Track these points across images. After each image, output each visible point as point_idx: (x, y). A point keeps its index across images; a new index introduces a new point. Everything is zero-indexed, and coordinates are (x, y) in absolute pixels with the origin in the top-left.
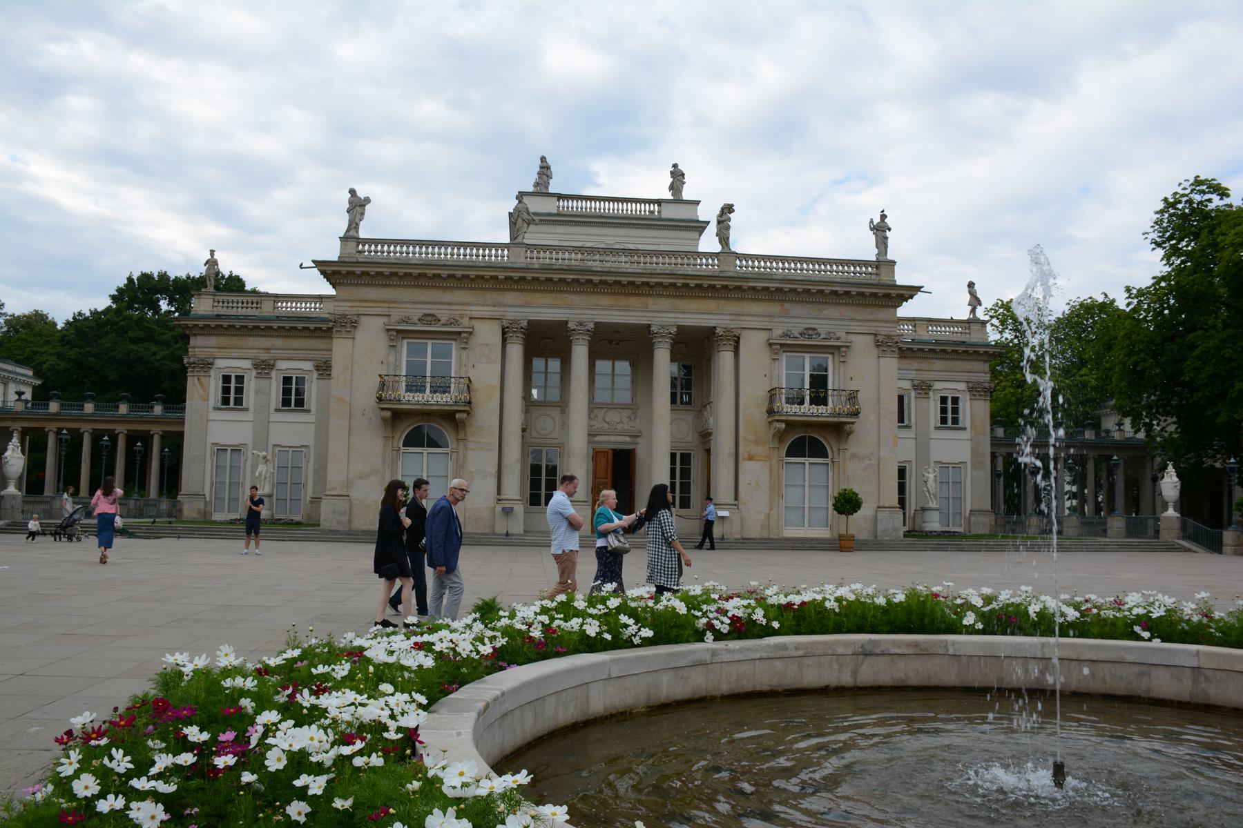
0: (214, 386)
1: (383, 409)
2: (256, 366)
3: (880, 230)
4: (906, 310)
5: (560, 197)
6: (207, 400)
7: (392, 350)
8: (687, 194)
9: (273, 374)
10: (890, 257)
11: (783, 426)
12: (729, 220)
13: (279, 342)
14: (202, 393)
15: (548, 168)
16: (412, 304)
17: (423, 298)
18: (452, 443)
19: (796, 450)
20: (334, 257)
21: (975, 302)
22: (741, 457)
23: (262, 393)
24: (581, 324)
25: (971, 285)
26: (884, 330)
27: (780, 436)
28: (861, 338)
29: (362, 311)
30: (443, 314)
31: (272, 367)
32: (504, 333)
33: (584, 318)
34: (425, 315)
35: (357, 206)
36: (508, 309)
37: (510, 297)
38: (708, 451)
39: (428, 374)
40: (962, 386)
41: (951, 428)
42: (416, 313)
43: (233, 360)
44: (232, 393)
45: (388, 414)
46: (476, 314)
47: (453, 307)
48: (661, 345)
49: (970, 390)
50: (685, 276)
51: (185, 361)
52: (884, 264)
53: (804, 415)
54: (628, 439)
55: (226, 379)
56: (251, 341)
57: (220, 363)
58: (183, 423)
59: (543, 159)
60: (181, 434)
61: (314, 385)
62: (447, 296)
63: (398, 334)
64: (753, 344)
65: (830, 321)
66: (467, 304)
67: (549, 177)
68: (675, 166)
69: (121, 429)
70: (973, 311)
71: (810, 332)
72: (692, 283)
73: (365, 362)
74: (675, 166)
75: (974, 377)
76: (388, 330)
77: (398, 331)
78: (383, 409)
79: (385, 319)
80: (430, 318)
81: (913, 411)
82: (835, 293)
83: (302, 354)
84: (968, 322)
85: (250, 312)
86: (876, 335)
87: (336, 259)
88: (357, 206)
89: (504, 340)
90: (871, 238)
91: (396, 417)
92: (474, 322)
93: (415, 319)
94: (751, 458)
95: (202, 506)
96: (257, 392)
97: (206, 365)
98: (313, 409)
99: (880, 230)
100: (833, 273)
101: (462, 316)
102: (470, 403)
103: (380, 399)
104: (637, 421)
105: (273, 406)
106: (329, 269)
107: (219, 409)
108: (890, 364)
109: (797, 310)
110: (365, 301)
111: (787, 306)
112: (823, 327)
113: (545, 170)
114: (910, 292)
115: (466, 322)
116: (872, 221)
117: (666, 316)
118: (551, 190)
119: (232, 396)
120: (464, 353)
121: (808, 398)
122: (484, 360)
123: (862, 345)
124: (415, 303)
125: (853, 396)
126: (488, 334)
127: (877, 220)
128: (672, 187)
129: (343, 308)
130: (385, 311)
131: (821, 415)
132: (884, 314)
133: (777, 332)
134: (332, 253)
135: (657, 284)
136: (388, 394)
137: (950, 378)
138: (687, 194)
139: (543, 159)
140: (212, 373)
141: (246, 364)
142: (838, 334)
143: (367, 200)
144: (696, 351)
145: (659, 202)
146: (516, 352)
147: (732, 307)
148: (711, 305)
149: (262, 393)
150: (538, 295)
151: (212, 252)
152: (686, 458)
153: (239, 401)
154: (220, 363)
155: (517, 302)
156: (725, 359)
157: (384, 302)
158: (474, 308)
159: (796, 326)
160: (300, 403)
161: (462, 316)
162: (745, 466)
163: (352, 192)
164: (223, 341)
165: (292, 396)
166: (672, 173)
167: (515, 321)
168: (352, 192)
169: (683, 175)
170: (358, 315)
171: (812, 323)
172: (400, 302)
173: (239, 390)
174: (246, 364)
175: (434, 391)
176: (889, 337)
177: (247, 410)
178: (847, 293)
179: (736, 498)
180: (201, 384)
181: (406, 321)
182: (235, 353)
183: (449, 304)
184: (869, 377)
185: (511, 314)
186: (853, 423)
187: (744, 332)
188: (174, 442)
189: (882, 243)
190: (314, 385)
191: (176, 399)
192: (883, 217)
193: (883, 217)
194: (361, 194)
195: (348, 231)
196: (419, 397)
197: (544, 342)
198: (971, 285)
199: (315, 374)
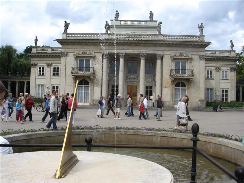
0: (38, 70)
1: (73, 76)
2: (47, 65)
3: (201, 27)
4: (206, 49)
5: (121, 21)
7: (76, 61)
8: (154, 19)
11: (173, 79)
12: (161, 26)
14: (34, 72)
15: (118, 13)
16: (80, 50)
18: (90, 84)
19: (177, 85)
20: (61, 38)
21: (232, 46)
23: (48, 71)
24: (122, 53)
25: (231, 41)
26: (202, 54)
27: (173, 82)
28: (195, 56)
29: (68, 51)
30: (88, 51)
32: (103, 56)
33: (123, 52)
34: (83, 52)
35: (67, 25)
39: (84, 67)
40: (213, 68)
41: (225, 79)
43: (42, 63)
44: (42, 71)
45: (74, 77)
47: (90, 50)
49: (231, 69)
51: (30, 64)
52: (202, 36)
53: (179, 76)
55: (40, 68)
56: (45, 59)
57: (39, 64)
58: (30, 79)
59: (117, 11)
60: (30, 81)
63: (77, 57)
65: (187, 53)
67: (118, 16)
68: (151, 12)
69: (17, 81)
70: (232, 48)
71: (181, 55)
72: (150, 42)
73: (69, 64)
74: (151, 12)
75: (231, 66)
76: (74, 56)
77: (77, 56)
78: (73, 76)
79: (74, 53)
81: (220, 75)
82: (198, 45)
84: (230, 51)
85: (45, 52)
87: (62, 38)
88: (67, 25)
89: (103, 58)
90: (198, 30)
91: (76, 78)
92: (96, 54)
93: (81, 53)
94: (165, 87)
97: (35, 65)
99: (201, 27)
100: (188, 39)
102: (94, 74)
103: (72, 73)
106: (60, 41)
107: (39, 76)
108: (203, 63)
113: (117, 14)
114: (209, 43)
116: (198, 25)
117: (145, 51)
118: (119, 19)
119: (41, 72)
120: (93, 61)
121: (181, 72)
122: (98, 63)
123: (196, 58)
125: (192, 71)
126: (99, 56)
127: (200, 25)
128: (150, 17)
129: (63, 51)
130: (74, 51)
131: (184, 76)
132: (201, 49)
133: (173, 55)
134: (60, 37)
135: (141, 43)
136: (74, 72)
137: (225, 66)
138: (154, 19)
139: (117, 11)
141: (45, 65)
142: (189, 55)
143: (69, 24)
144: (151, 60)
145: (147, 21)
146: (105, 60)
149: (48, 71)
151: (36, 37)
152: (151, 87)
153: (43, 74)
154: (39, 64)
156: (159, 62)
159: (178, 53)
162: (164, 89)
163: (66, 22)
165: (56, 72)
166: (150, 13)
168: (66, 22)
169: (153, 14)
170: (67, 52)
171: (182, 52)
173: (43, 71)
174: (45, 65)
175: (85, 71)
176: (203, 55)
177: (44, 76)
180: (34, 70)
181: (79, 54)
184: (198, 68)
186: (192, 78)
187: (165, 55)
188: (29, 83)
189: (202, 31)
191: (29, 74)
192: (202, 24)
193: (202, 24)
194: (68, 22)
195: (64, 31)
196: (81, 72)
198: (231, 41)
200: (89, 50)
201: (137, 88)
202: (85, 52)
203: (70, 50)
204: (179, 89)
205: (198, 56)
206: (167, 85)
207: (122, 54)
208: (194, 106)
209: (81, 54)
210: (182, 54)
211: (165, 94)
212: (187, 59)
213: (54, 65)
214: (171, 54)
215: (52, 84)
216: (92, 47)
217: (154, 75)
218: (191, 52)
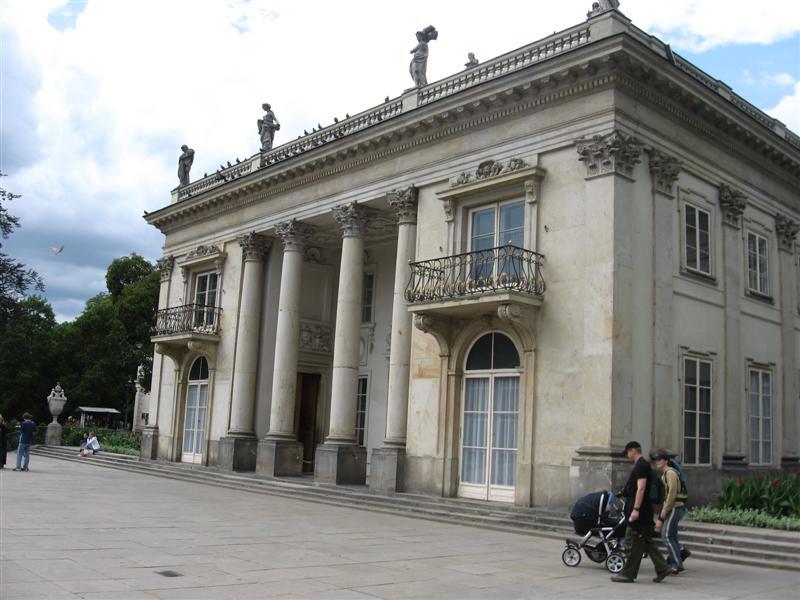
17: (204, 231)
35: (187, 158)
37: (249, 213)
64: (432, 210)
71: (486, 169)
80: (202, 250)
88: (187, 158)
89: (244, 257)
94: (421, 375)
112: (502, 156)
123: (565, 166)
126: (235, 253)
142: (527, 160)
178: (519, 93)
202: (202, 247)
204: (486, 380)
205: (573, 155)
208: (550, 494)
210: (492, 162)
211: (418, 413)
212: (514, 189)
214: (447, 181)
218: (538, 139)
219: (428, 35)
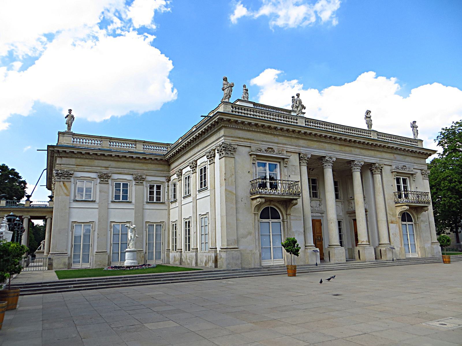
2: (100, 177)
6: (68, 195)
9: (110, 181)
10: (419, 137)
13: (113, 164)
16: (263, 142)
22: (389, 222)
24: (330, 158)
31: (108, 177)
34: (269, 148)
36: (301, 148)
37: (301, 142)
38: (355, 220)
42: (264, 146)
46: (289, 150)
47: (279, 145)
48: (358, 170)
50: (156, 155)
54: (320, 215)
56: (96, 162)
61: (134, 188)
62: (276, 139)
66: (285, 144)
83: (126, 171)
86: (421, 170)
92: (289, 154)
94: (392, 223)
95: (66, 260)
96: (100, 191)
98: (133, 201)
99: (414, 125)
101: (283, 150)
104: (322, 206)
105: (110, 200)
109: (398, 157)
110: (239, 138)
111: (395, 155)
115: (285, 152)
122: (293, 173)
124: (263, 141)
140: (72, 180)
147: (379, 154)
148: (372, 153)
150: (312, 143)
155: (304, 145)
156: (378, 177)
157: (248, 139)
158: (288, 147)
160: (125, 197)
161: (283, 150)
162: (391, 225)
164: (79, 161)
167: (306, 155)
172: (256, 140)
179: (390, 242)
180: (65, 186)
182: (87, 168)
183: (278, 143)
185: (303, 151)
189: (416, 133)
190: (134, 188)
197: (315, 167)
199: (134, 182)
200: (276, 145)
201: (321, 224)
203: (242, 140)
206: (394, 219)
207: (330, 160)
209: (263, 152)
213: (115, 176)
215: (112, 222)
216: (281, 139)
217: (352, 199)
219: (368, 112)
